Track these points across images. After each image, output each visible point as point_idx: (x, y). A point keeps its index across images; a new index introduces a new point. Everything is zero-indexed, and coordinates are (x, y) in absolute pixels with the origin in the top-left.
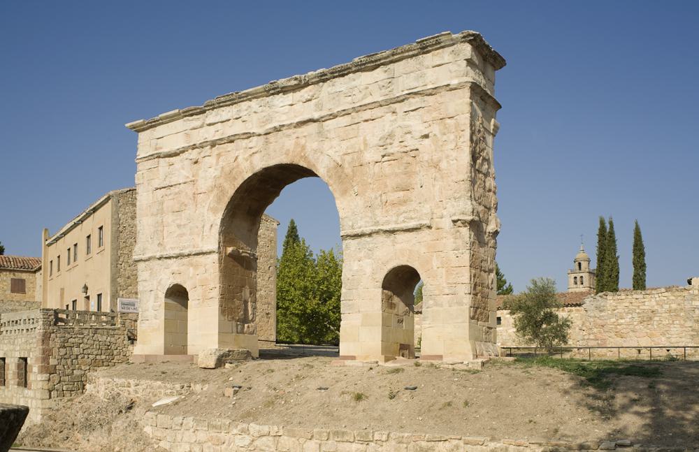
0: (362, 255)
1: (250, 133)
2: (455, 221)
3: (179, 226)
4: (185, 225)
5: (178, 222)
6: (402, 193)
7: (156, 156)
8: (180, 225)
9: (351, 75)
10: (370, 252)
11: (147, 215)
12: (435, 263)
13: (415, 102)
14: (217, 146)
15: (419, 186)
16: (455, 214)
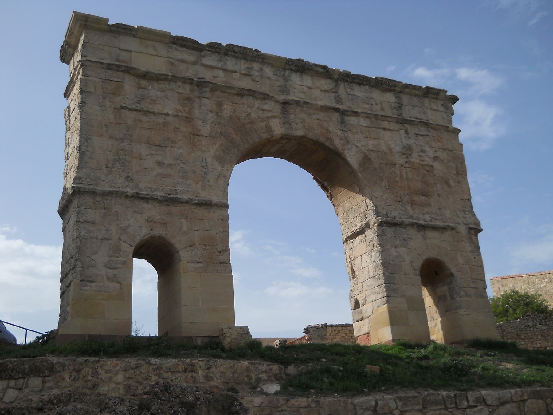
0: (398, 242)
1: (268, 95)
2: (470, 229)
3: (160, 164)
4: (170, 165)
5: (160, 158)
6: (423, 198)
7: (123, 69)
8: (163, 163)
9: (367, 87)
10: (404, 242)
11: (101, 136)
12: (460, 260)
13: (423, 130)
14: (219, 92)
15: (436, 195)
16: (471, 224)
